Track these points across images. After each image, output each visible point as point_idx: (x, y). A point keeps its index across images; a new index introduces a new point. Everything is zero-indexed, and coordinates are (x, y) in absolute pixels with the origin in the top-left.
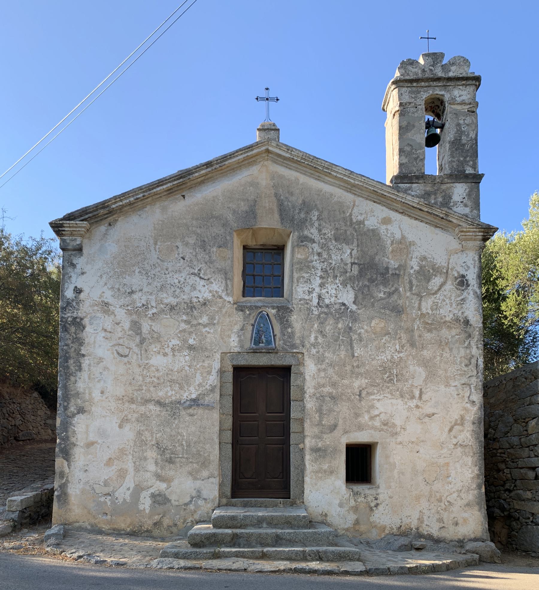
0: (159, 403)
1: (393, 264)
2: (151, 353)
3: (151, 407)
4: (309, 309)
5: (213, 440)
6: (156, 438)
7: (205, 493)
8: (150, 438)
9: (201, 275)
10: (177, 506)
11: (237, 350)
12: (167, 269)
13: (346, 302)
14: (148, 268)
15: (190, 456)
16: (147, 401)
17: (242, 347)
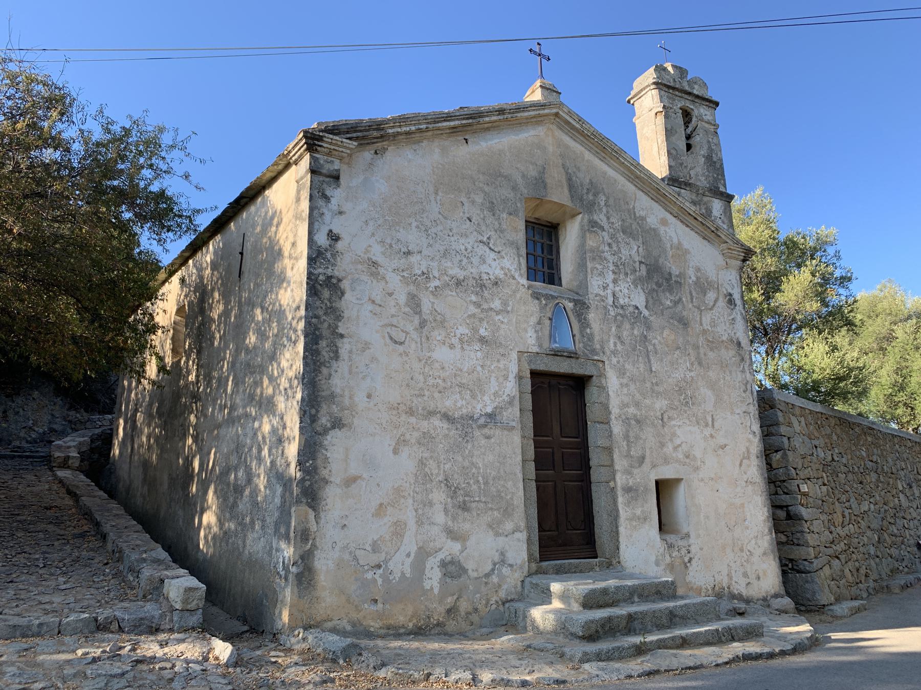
0: (446, 417)
1: (675, 271)
2: (435, 342)
3: (436, 422)
4: (605, 308)
5: (515, 475)
6: (444, 471)
7: (511, 557)
8: (437, 471)
9: (491, 245)
10: (476, 578)
11: (535, 349)
12: (450, 230)
13: (638, 305)
14: (429, 224)
15: (489, 500)
16: (431, 413)
17: (540, 346)
